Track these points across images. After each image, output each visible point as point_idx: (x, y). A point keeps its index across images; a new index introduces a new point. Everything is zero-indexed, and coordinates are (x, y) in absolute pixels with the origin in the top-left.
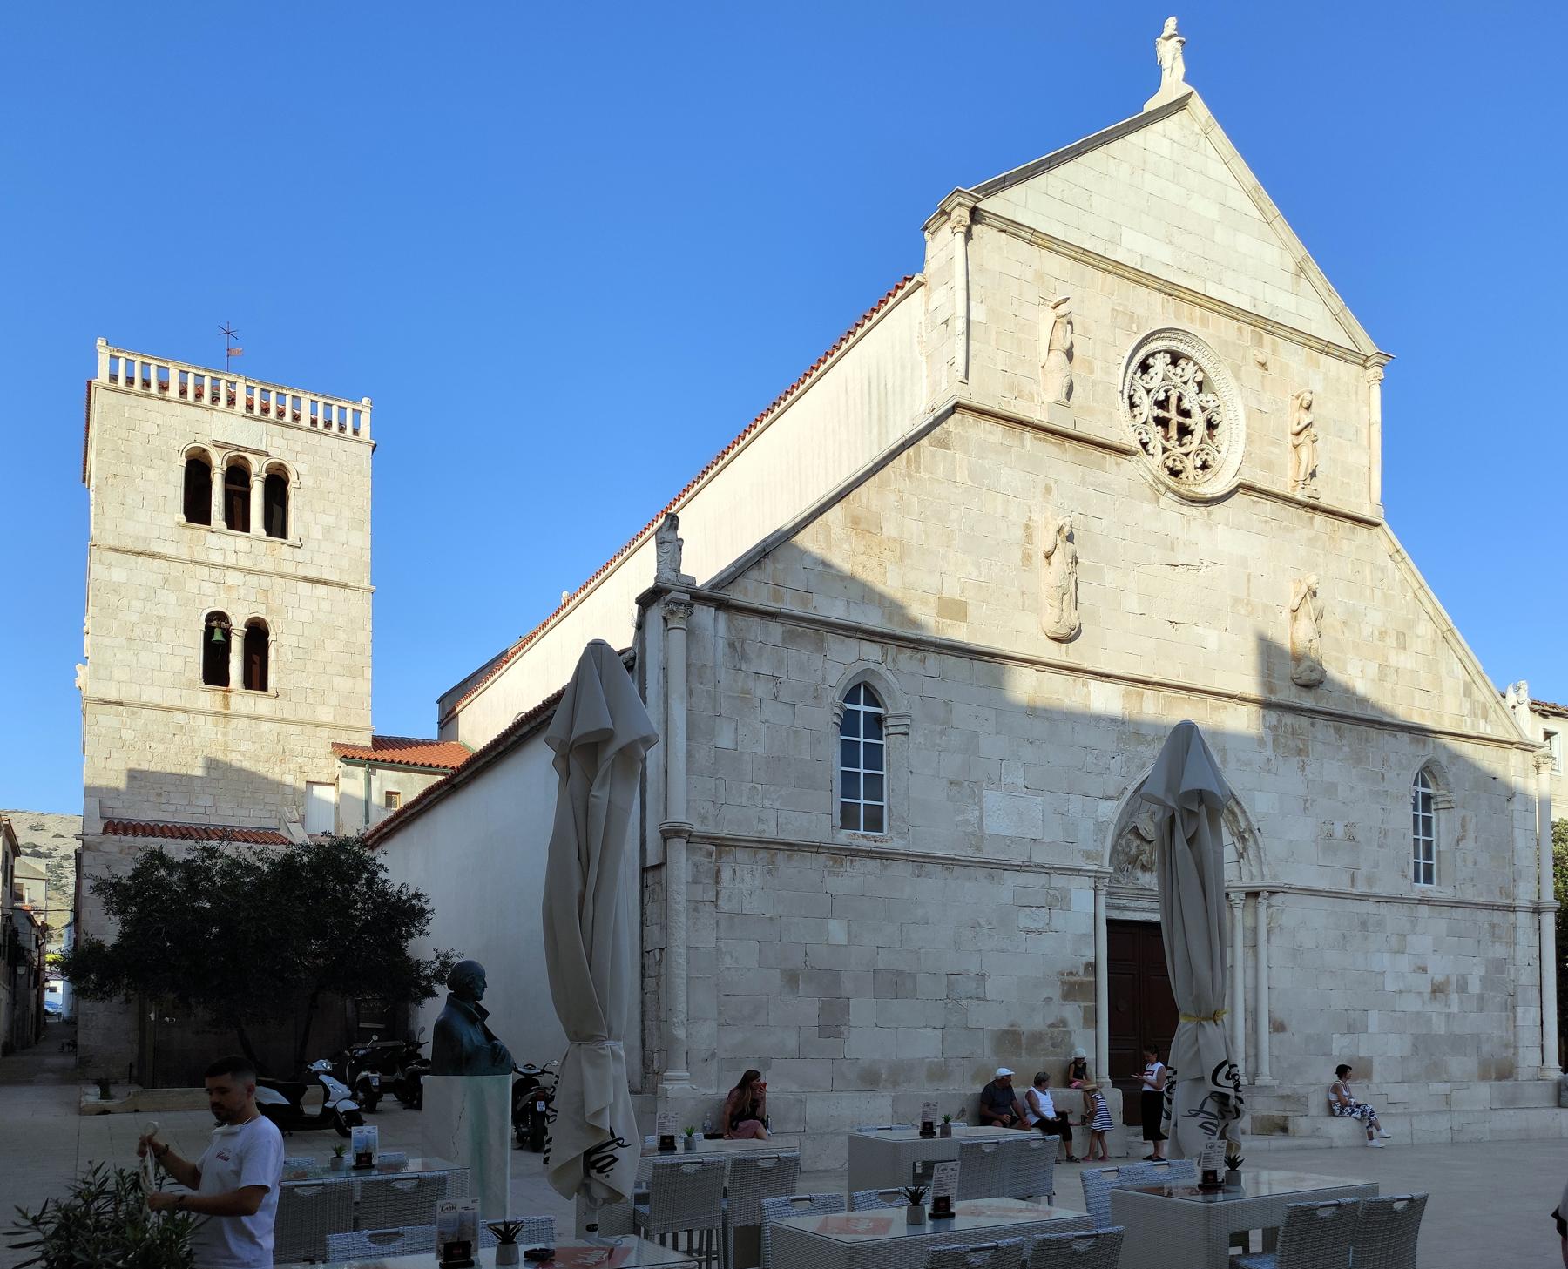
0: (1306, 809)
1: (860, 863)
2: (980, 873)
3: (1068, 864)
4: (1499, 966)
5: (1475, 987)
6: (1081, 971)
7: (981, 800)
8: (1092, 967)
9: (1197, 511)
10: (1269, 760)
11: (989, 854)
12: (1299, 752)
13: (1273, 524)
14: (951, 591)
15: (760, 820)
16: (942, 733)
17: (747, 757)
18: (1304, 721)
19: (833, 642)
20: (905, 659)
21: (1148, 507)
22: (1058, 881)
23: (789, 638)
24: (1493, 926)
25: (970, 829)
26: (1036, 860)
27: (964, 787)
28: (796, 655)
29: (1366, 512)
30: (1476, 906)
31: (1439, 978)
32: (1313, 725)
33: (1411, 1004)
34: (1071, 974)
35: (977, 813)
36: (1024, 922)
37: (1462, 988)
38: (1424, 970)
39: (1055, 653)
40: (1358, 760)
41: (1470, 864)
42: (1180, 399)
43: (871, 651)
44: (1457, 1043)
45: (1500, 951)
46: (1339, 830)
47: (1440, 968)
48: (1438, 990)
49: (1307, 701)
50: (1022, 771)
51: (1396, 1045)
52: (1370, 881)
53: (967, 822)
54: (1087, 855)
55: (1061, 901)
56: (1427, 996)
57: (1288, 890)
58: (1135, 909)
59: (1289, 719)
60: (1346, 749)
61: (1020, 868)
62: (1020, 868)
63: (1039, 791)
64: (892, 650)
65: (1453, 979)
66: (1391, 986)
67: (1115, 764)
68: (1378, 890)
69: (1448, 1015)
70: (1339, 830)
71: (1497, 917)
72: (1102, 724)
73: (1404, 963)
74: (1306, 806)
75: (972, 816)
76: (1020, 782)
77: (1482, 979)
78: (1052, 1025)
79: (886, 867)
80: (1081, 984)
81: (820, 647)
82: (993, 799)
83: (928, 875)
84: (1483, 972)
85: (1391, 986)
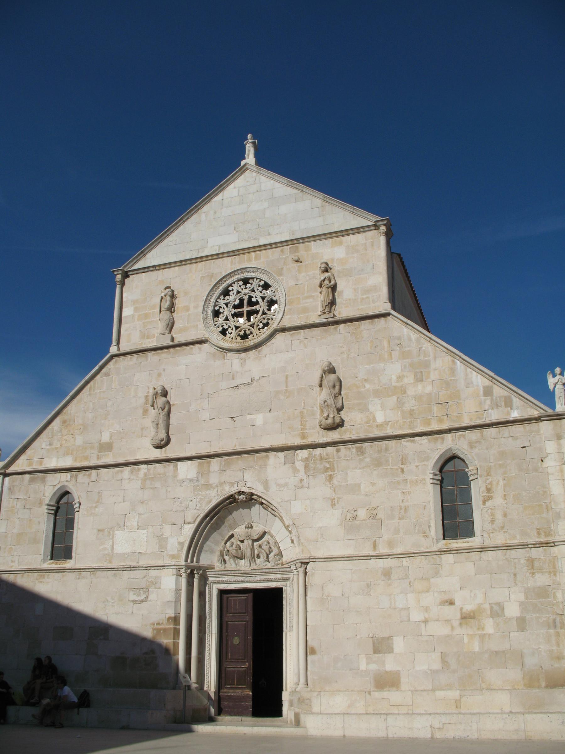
0: (333, 505)
1: (52, 575)
2: (110, 573)
3: (160, 563)
4: (543, 592)
5: (513, 610)
6: (165, 622)
7: (113, 537)
8: (176, 620)
9: (252, 353)
10: (302, 480)
11: (115, 564)
12: (326, 470)
13: (306, 341)
14: (105, 438)
15: (12, 561)
16: (96, 507)
17: (10, 535)
18: (330, 450)
19: (50, 476)
20: (82, 476)
21: (218, 363)
22: (153, 573)
23: (32, 480)
24: (531, 561)
25: (106, 552)
26: (142, 563)
27: (105, 532)
28: (36, 486)
29: (380, 311)
30: (506, 547)
31: (469, 608)
32: (338, 451)
33: (438, 629)
34: (159, 624)
35: (111, 543)
36: (132, 597)
37: (497, 611)
38: (452, 603)
39: (157, 454)
40: (378, 463)
41: (499, 516)
42: (250, 297)
43: (65, 477)
44: (499, 658)
45: (541, 580)
46: (362, 514)
47: (467, 601)
48: (467, 618)
49: (334, 436)
50: (137, 518)
51: (428, 662)
52: (390, 544)
53: (105, 549)
54: (173, 557)
55: (156, 583)
56: (456, 623)
57: (314, 560)
58: (235, 582)
59: (318, 451)
60: (368, 460)
61: (130, 568)
62: (130, 568)
63: (145, 527)
64: (74, 473)
65: (487, 606)
66: (416, 616)
67: (192, 505)
68: (399, 550)
69: (482, 637)
70: (362, 514)
71: (536, 553)
72: (185, 483)
73: (428, 599)
74: (333, 503)
75: (108, 545)
76: (135, 524)
77: (521, 604)
78: (146, 653)
79: (63, 576)
80: (165, 630)
81: (43, 480)
82: (119, 534)
83: (83, 578)
84: (522, 597)
85: (416, 616)
